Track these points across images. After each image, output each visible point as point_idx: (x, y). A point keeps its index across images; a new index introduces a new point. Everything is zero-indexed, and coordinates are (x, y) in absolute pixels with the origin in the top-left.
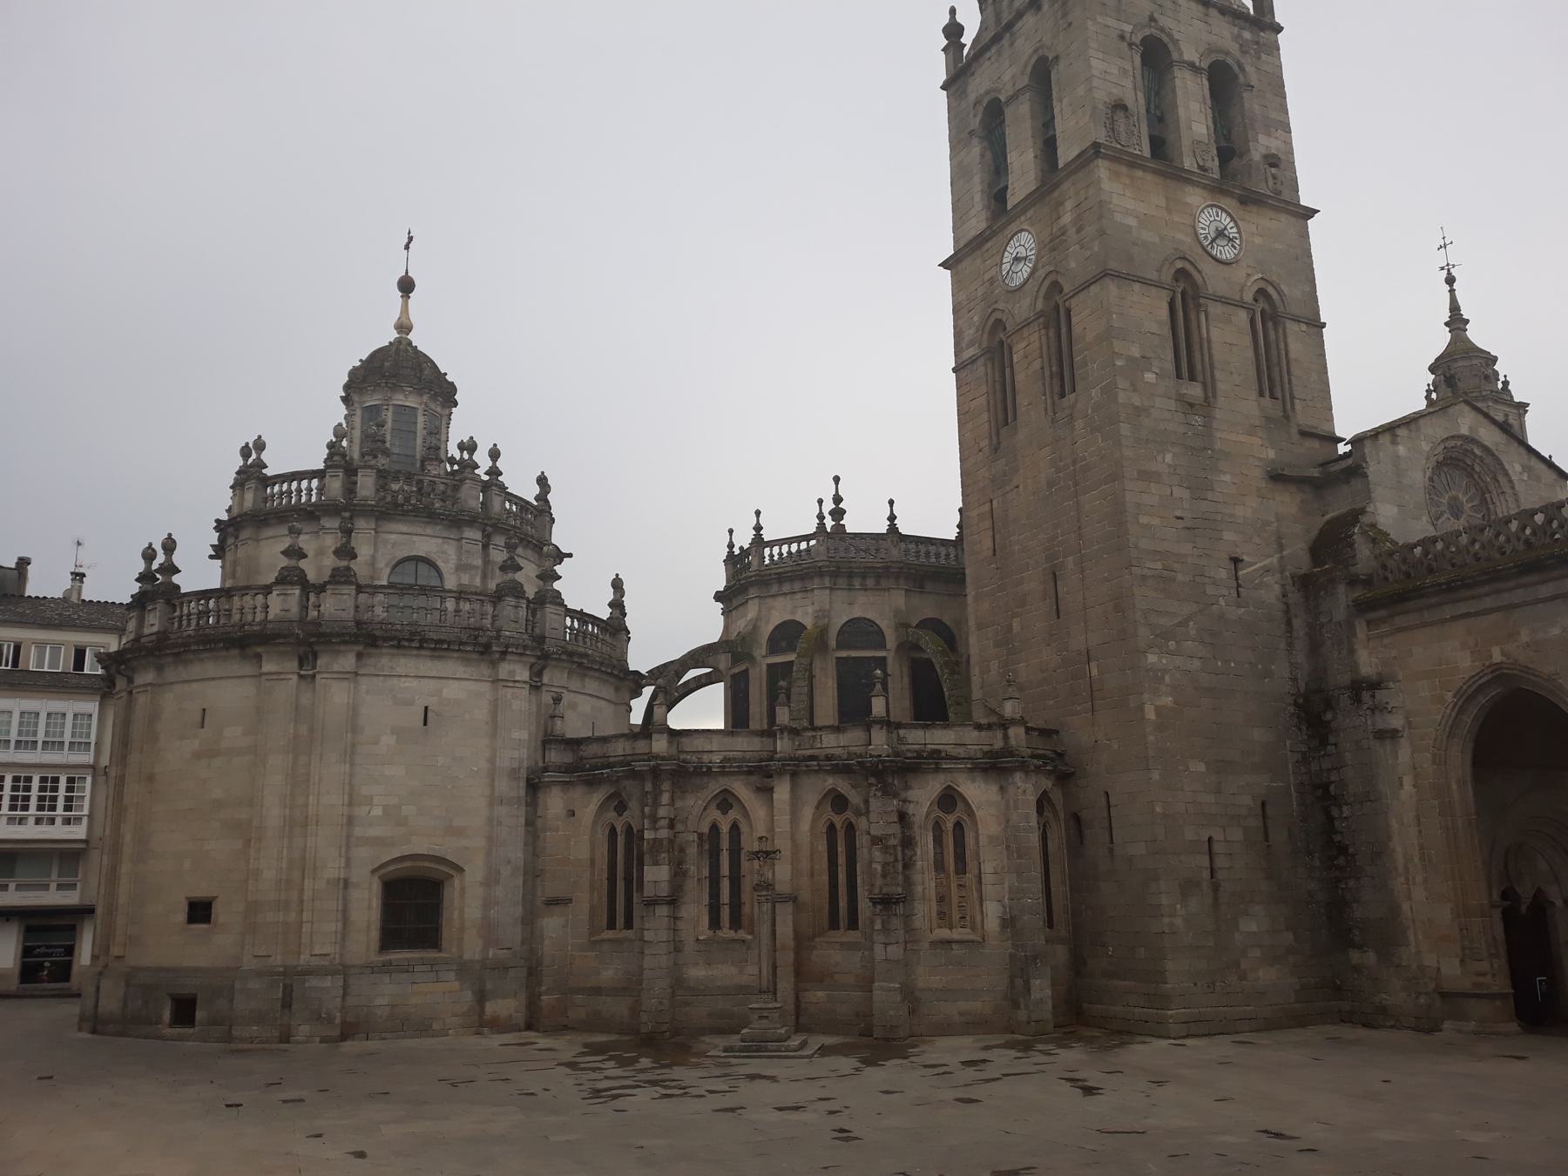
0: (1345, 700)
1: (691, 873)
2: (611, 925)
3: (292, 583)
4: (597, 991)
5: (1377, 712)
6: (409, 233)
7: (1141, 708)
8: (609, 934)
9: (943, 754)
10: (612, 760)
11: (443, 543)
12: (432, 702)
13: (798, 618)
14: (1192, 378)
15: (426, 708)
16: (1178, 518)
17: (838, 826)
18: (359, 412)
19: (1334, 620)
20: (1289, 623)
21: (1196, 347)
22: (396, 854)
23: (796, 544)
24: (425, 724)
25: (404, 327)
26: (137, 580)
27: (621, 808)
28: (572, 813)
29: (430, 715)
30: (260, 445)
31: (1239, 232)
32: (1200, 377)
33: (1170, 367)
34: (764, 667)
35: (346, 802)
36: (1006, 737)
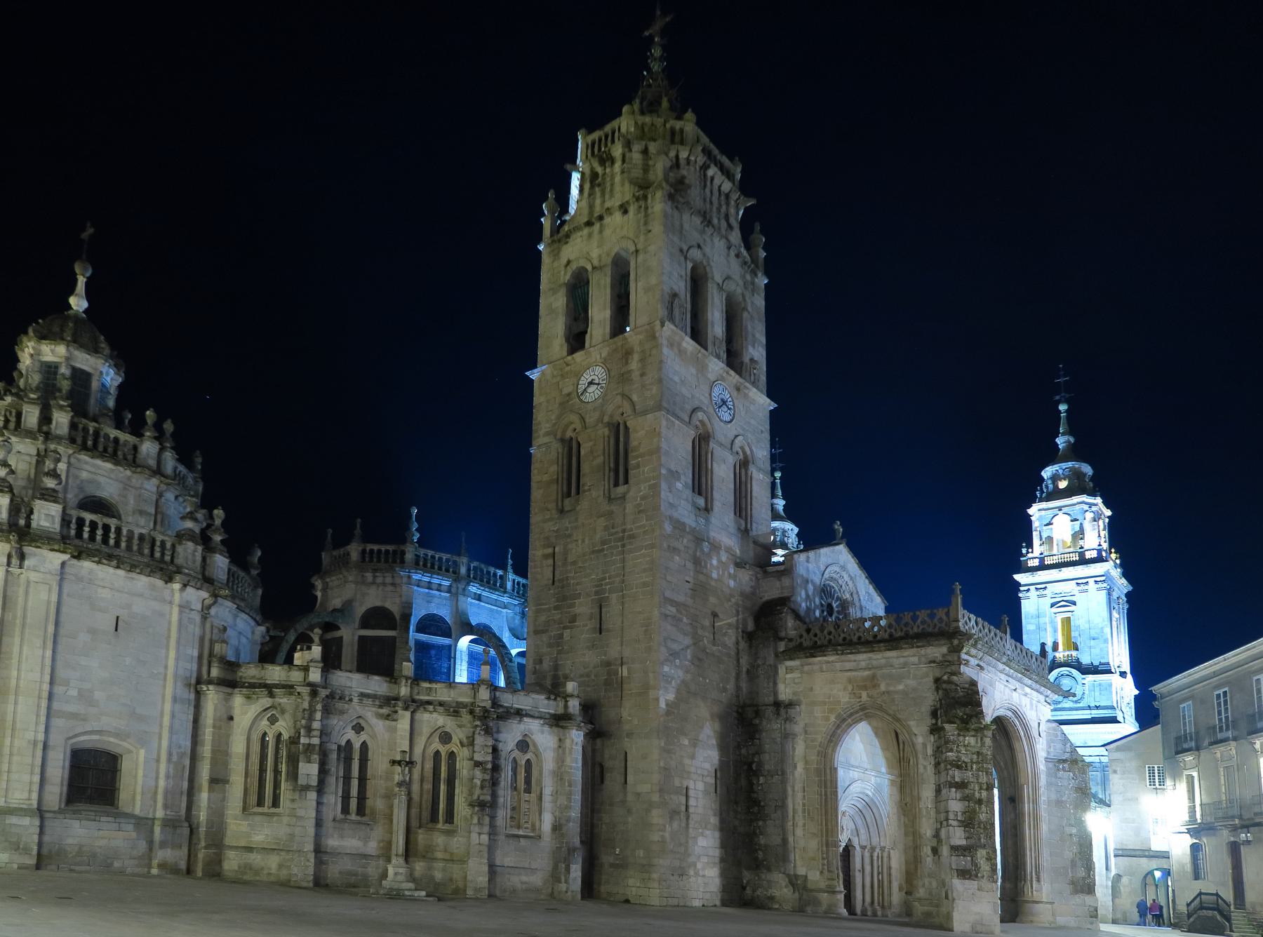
0: (770, 711)
1: (332, 772)
5: (788, 722)
7: (657, 700)
9: (524, 712)
14: (700, 494)
16: (687, 582)
17: (443, 754)
19: (767, 663)
20: (738, 661)
21: (703, 473)
27: (273, 720)
31: (733, 405)
32: (704, 495)
33: (690, 482)
36: (566, 707)
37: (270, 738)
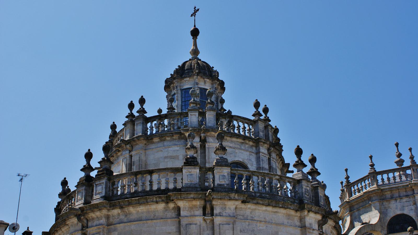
6: (195, 8)
11: (250, 155)
13: (406, 212)
18: (179, 92)
25: (195, 52)
26: (82, 170)
30: (142, 101)
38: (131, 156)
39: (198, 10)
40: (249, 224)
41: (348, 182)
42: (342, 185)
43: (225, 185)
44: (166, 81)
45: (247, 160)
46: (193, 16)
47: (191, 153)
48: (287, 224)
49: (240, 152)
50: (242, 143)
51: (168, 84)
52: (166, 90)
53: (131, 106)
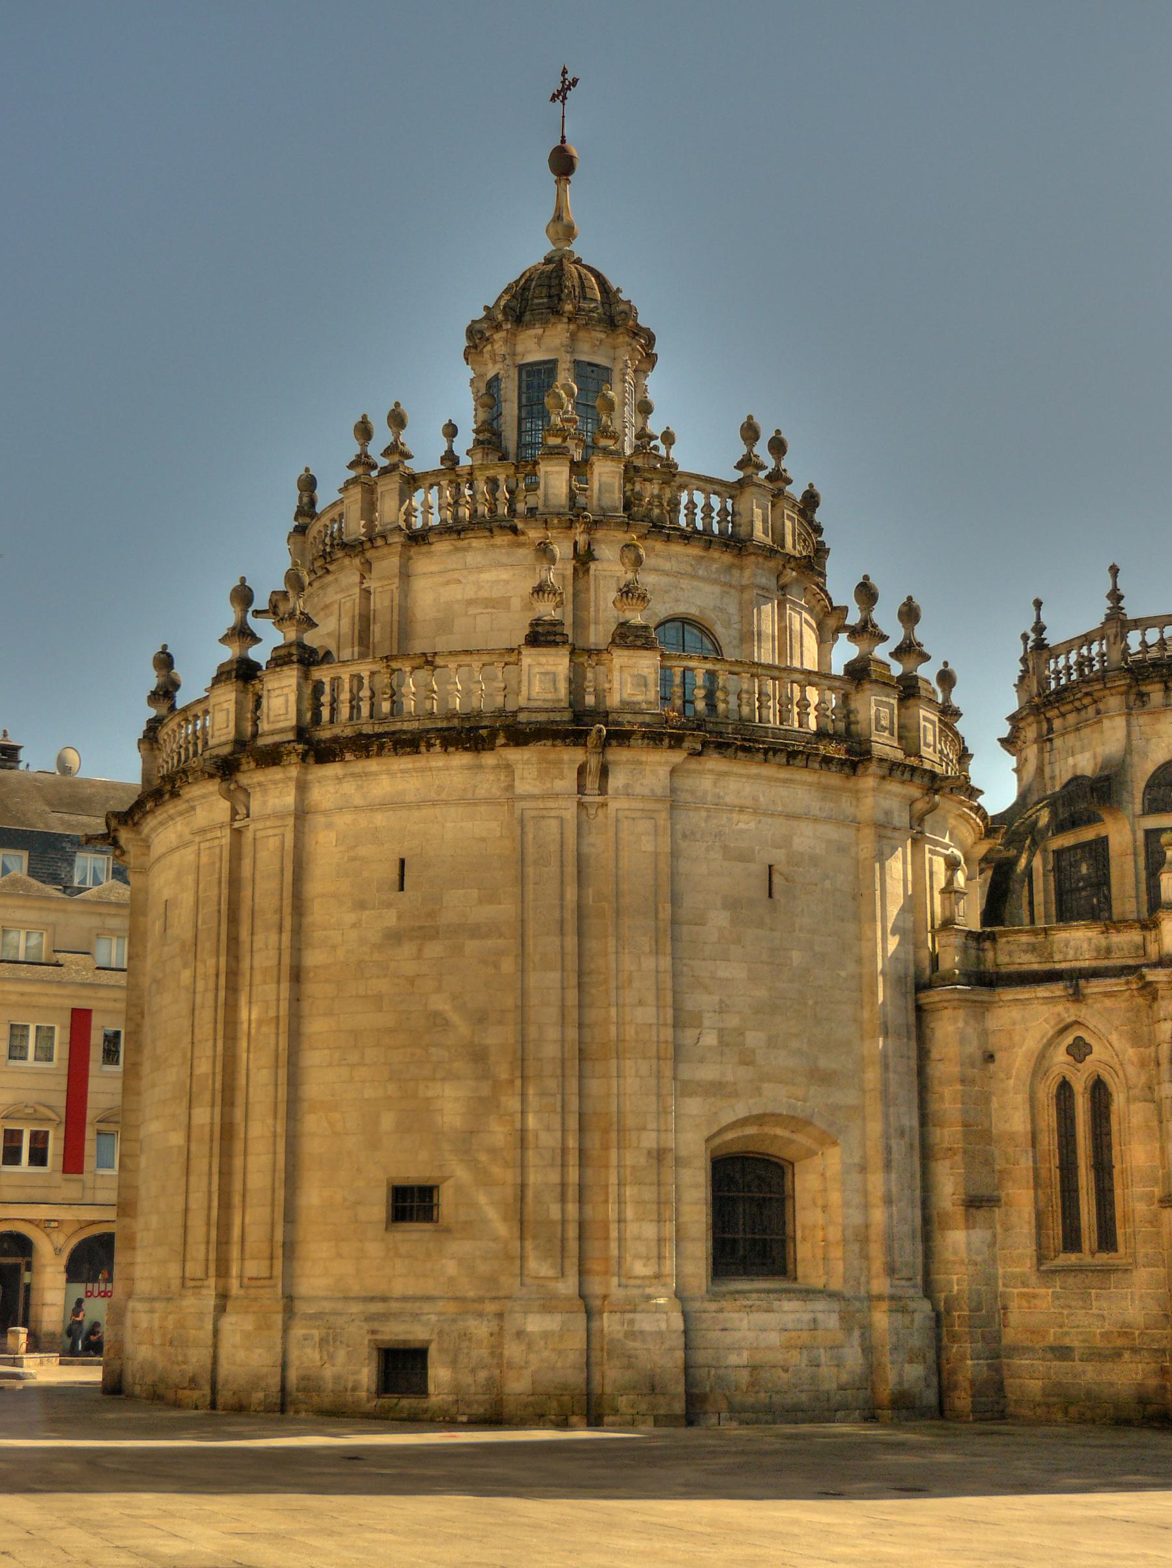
2: (1072, 1241)
3: (555, 644)
4: (1062, 1352)
6: (564, 72)
8: (1073, 1258)
10: (1057, 966)
12: (778, 856)
15: (770, 867)
22: (741, 1110)
23: (1157, 630)
24: (770, 896)
26: (224, 640)
28: (990, 1058)
29: (776, 879)
30: (397, 420)
34: (1141, 835)
35: (670, 1021)
37: (1080, 1087)
38: (367, 593)
39: (575, 82)
40: (709, 817)
41: (1040, 645)
42: (1026, 644)
43: (644, 706)
44: (471, 332)
45: (714, 609)
46: (558, 101)
47: (547, 609)
48: (817, 812)
49: (693, 588)
50: (702, 558)
51: (477, 338)
52: (470, 360)
53: (364, 431)
